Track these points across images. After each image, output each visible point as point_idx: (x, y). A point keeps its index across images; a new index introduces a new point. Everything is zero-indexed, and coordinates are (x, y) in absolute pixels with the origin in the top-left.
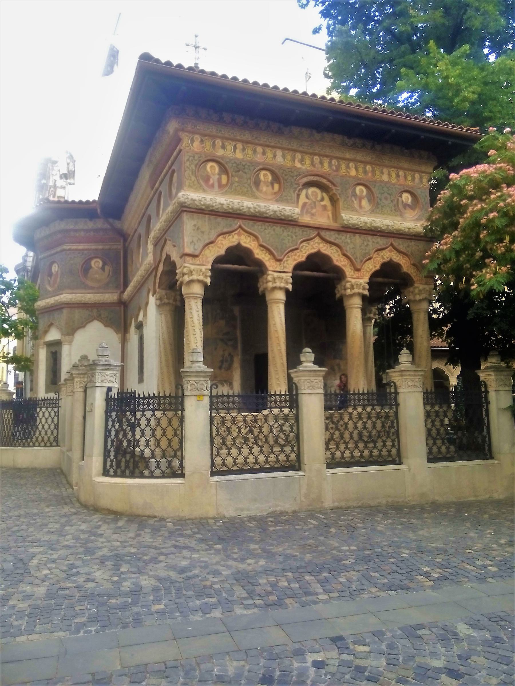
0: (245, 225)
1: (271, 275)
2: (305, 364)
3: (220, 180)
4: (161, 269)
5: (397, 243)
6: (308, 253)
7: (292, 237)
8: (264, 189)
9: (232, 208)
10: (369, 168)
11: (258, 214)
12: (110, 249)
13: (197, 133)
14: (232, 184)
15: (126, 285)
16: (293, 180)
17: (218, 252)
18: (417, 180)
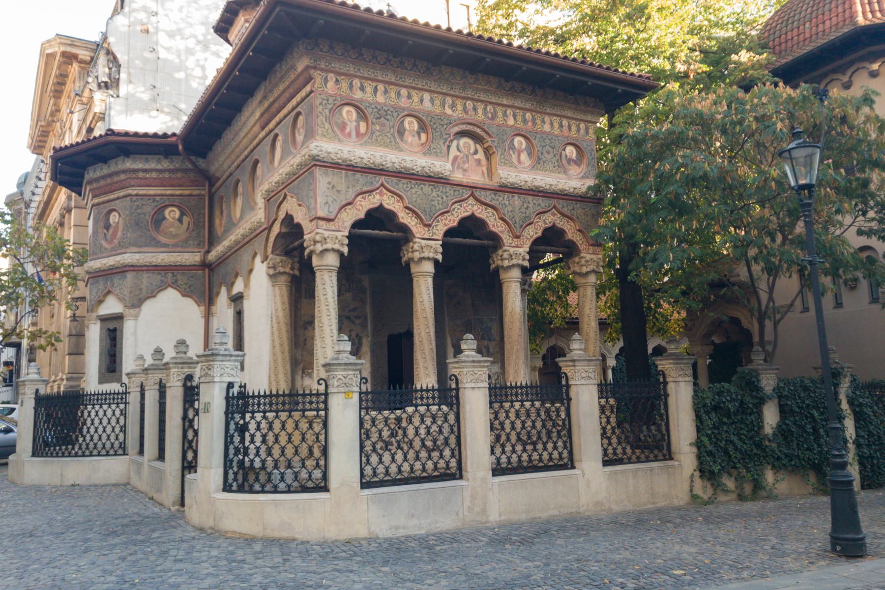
0: (388, 182)
1: (418, 243)
2: (466, 353)
3: (357, 128)
4: (276, 229)
5: (560, 204)
6: (460, 216)
7: (442, 198)
8: (410, 140)
9: (373, 163)
10: (528, 115)
11: (403, 170)
12: (190, 195)
13: (332, 72)
14: (373, 133)
15: (212, 241)
16: (442, 130)
17: (357, 215)
18: (582, 131)
